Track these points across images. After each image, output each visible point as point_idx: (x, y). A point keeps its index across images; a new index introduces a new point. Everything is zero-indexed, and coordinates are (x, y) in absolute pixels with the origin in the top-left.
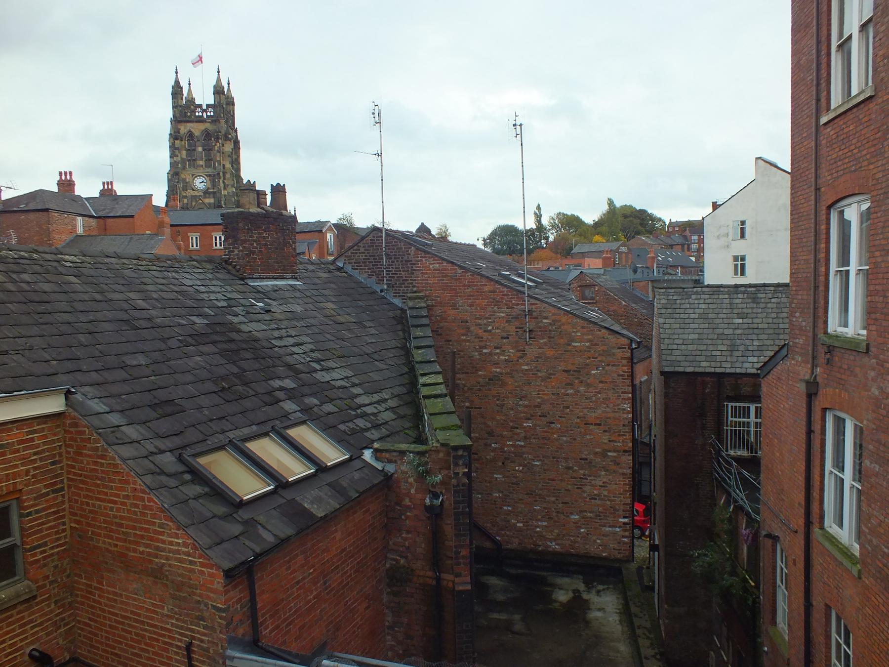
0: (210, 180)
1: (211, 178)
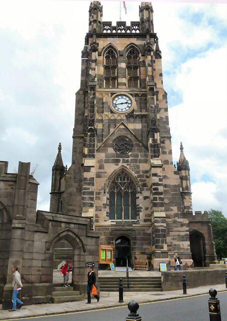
1: (137, 98)
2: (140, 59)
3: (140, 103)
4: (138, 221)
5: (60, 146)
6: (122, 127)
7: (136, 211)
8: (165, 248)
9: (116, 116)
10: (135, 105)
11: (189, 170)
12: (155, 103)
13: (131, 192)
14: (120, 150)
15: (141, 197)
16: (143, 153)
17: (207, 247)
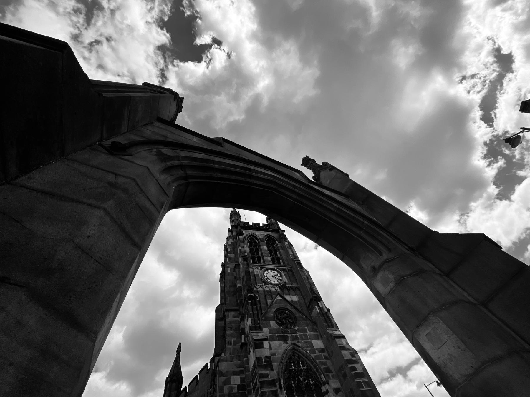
5: (180, 347)
6: (279, 298)
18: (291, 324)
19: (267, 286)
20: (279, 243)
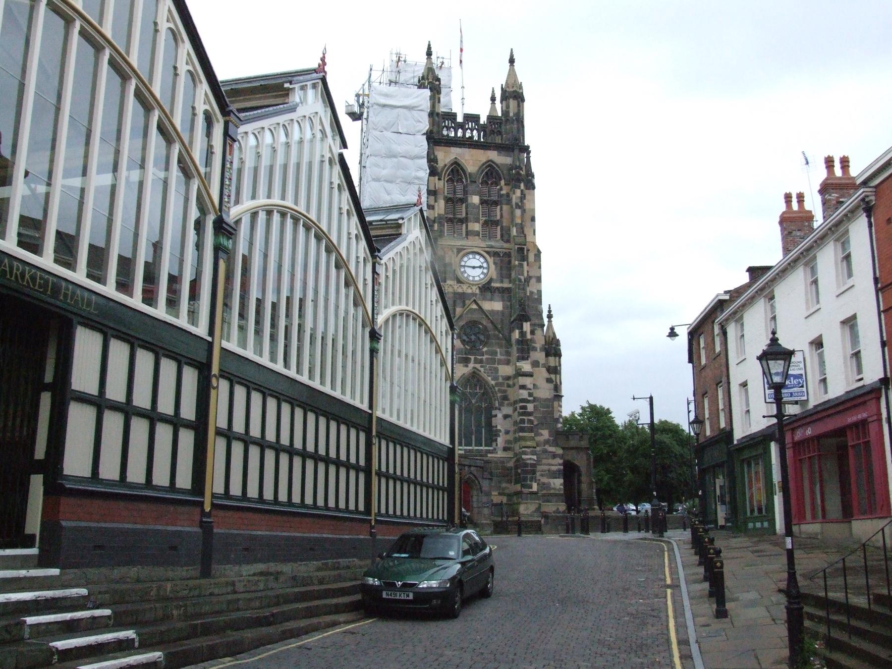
0: (495, 263)
2: (501, 189)
3: (501, 269)
4: (495, 449)
6: (474, 306)
7: (492, 435)
8: (535, 487)
9: (465, 287)
10: (493, 273)
11: (560, 356)
12: (526, 275)
13: (485, 407)
14: (471, 342)
15: (500, 416)
16: (504, 349)
17: (584, 486)
18: (481, 342)
19: (460, 286)
20: (505, 184)
